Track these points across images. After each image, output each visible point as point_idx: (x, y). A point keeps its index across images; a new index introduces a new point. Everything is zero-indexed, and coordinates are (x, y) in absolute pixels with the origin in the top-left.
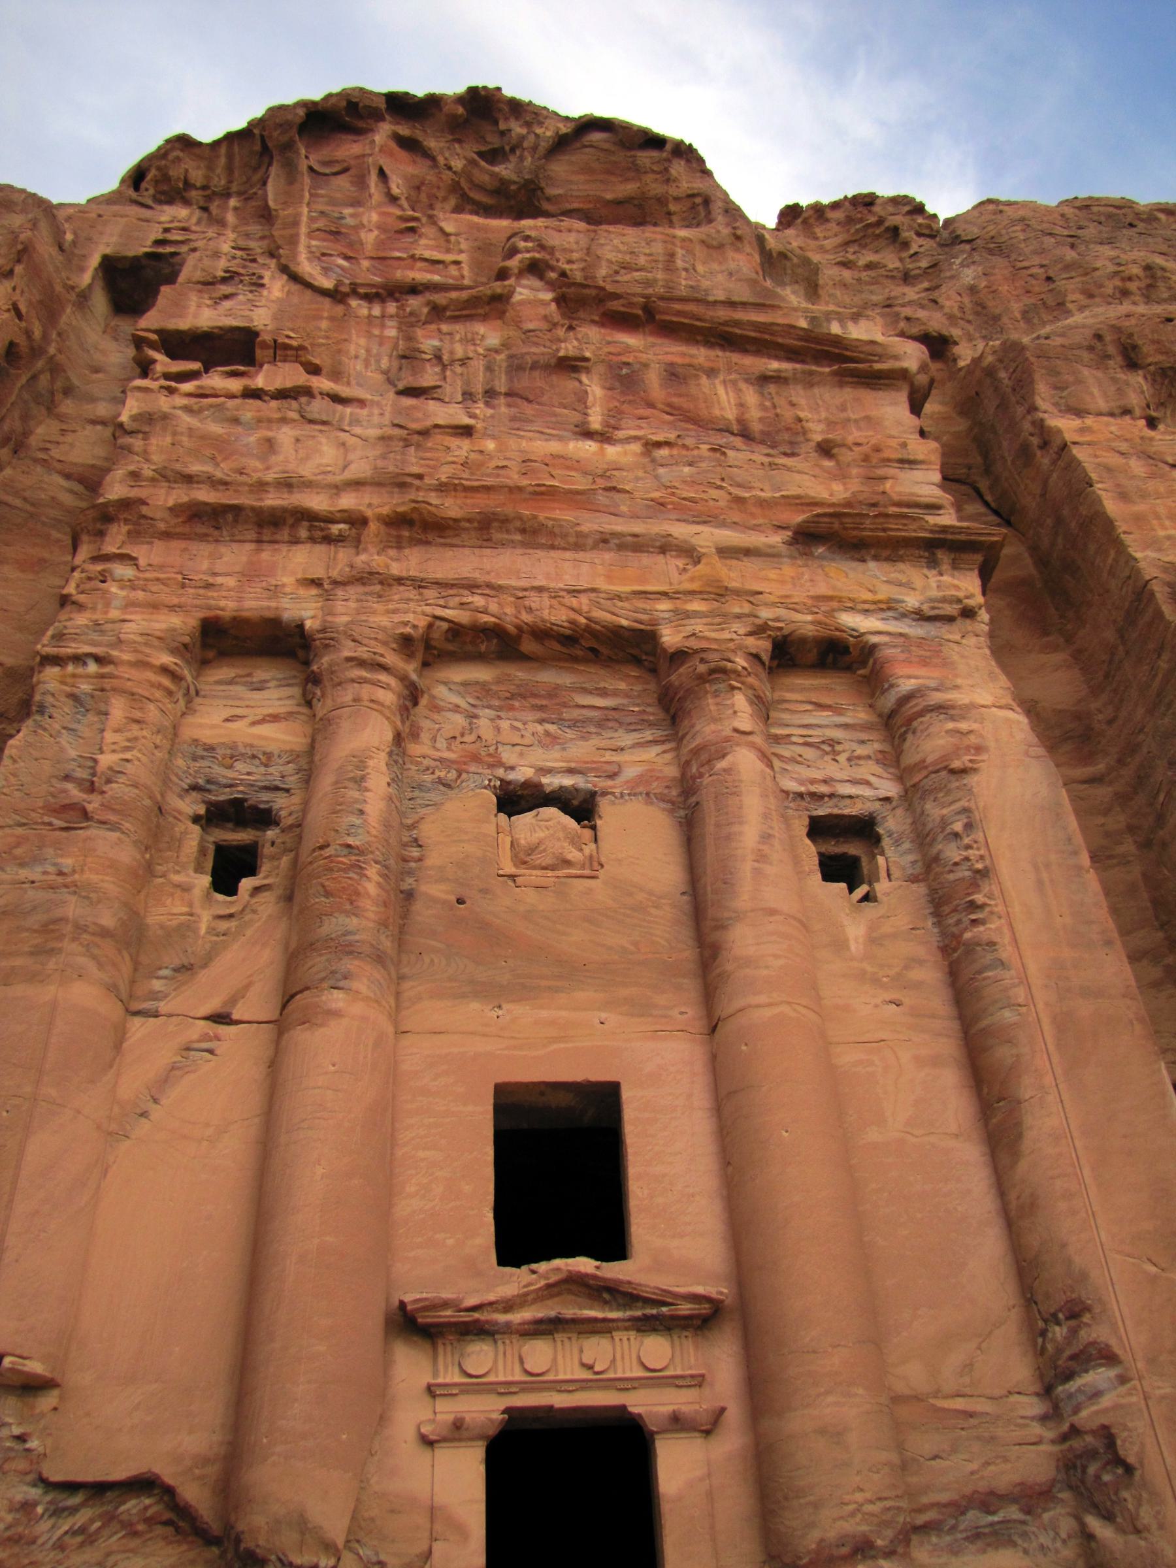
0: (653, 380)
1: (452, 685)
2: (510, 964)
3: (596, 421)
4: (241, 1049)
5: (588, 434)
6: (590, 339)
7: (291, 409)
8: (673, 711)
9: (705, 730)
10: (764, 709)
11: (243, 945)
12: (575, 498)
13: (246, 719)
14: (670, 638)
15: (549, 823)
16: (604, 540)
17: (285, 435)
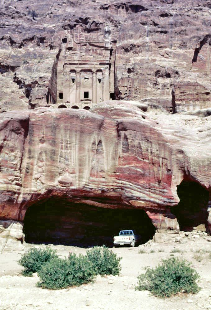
0: (95, 50)
1: (82, 73)
2: (85, 87)
3: (91, 54)
4: (75, 90)
5: (90, 55)
6: (91, 48)
7: (74, 54)
8: (92, 74)
9: (93, 76)
10: (96, 74)
11: (74, 85)
12: (89, 61)
13: (73, 74)
14: (92, 70)
15: (87, 80)
16: (90, 64)
17: (74, 56)
